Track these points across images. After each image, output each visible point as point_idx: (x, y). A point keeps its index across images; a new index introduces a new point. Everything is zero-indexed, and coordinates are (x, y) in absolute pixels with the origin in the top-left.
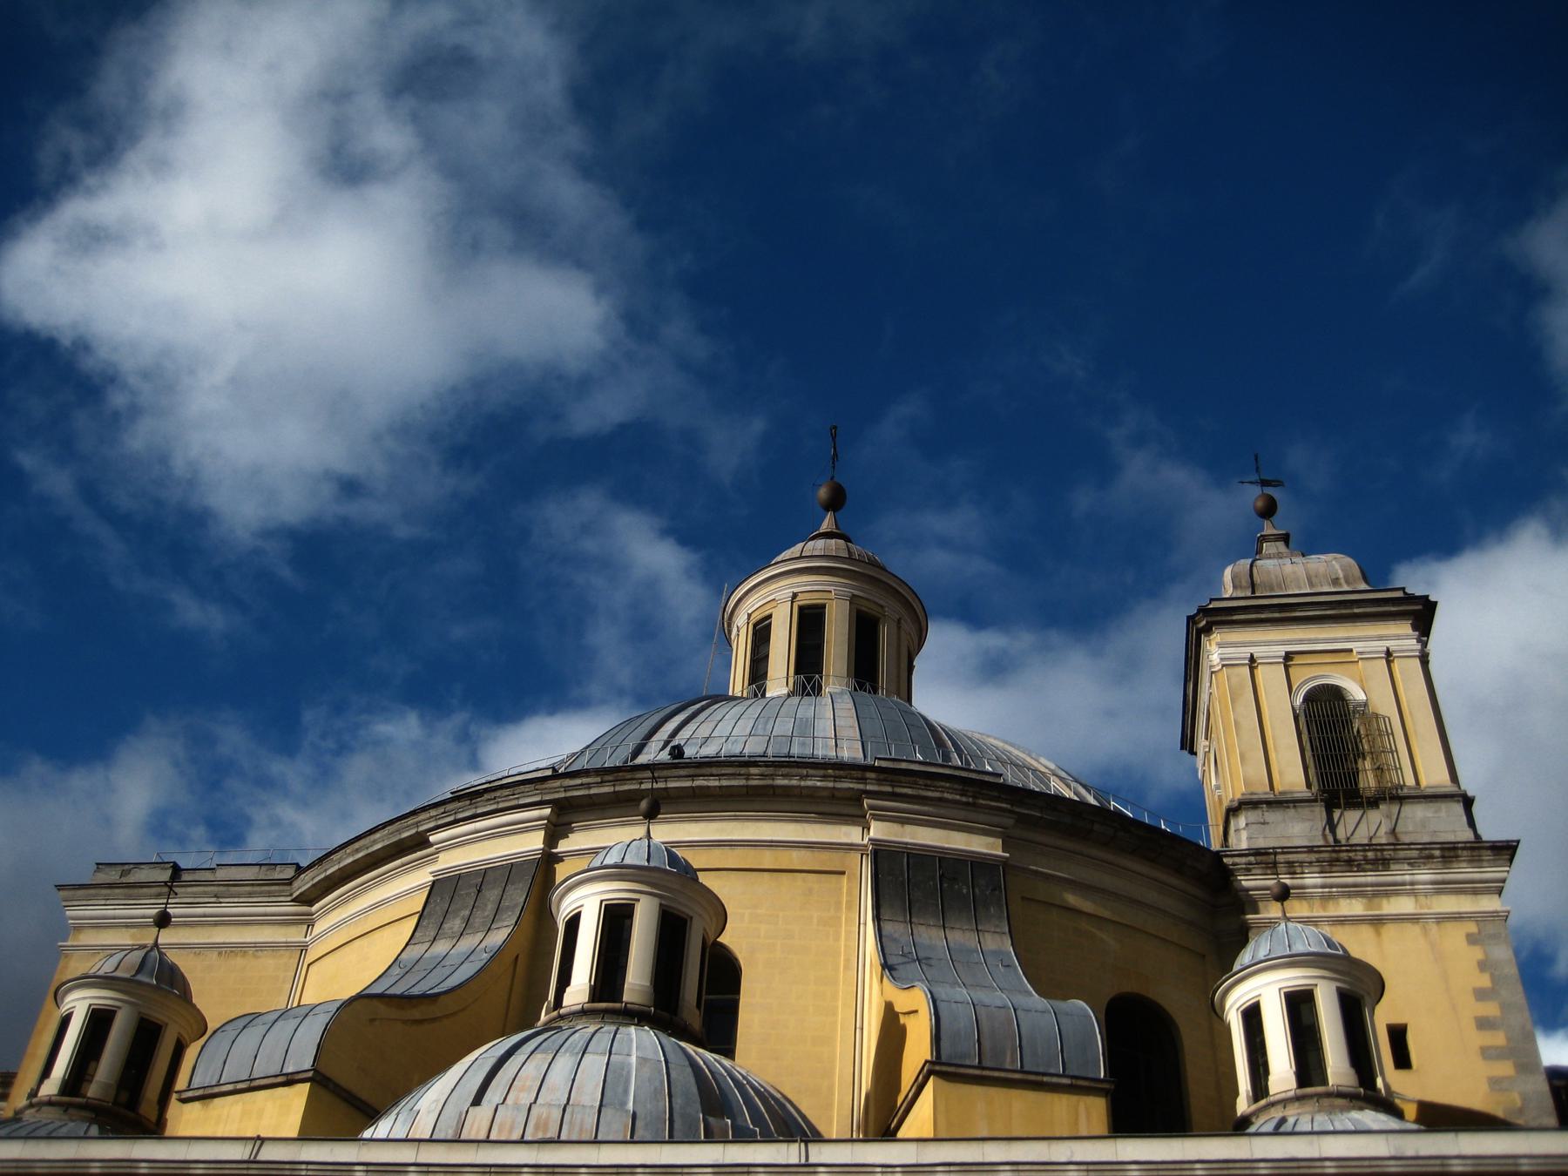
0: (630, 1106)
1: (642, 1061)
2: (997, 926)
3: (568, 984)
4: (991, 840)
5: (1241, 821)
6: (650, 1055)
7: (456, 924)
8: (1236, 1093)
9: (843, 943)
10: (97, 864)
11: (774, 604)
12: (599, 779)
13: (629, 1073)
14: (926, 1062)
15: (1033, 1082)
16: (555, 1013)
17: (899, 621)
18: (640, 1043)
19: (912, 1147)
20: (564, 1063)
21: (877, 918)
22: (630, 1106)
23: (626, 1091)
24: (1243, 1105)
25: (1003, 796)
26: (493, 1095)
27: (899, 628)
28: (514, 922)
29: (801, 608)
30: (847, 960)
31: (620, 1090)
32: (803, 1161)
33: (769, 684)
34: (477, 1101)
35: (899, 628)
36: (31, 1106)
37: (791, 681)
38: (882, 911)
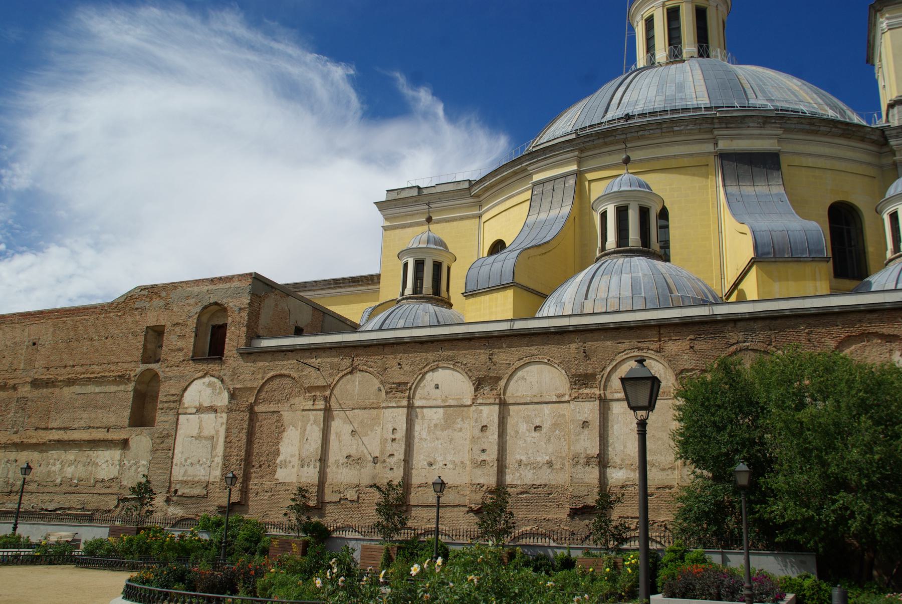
0: (643, 295)
1: (644, 275)
2: (777, 182)
3: (606, 240)
4: (772, 141)
5: (896, 110)
6: (646, 272)
7: (546, 205)
8: (886, 249)
9: (710, 196)
10: (387, 191)
11: (654, 8)
12: (597, 137)
13: (640, 280)
14: (752, 258)
15: (798, 261)
16: (603, 253)
17: (717, 6)
18: (641, 263)
19: (751, 305)
20: (615, 279)
21: (724, 185)
22: (643, 295)
23: (640, 288)
24: (889, 255)
25: (777, 121)
26: (591, 295)
27: (717, 9)
28: (571, 203)
29: (668, 9)
30: (713, 204)
31: (638, 288)
32: (711, 314)
33: (656, 52)
34: (586, 298)
35: (717, 9)
36: (403, 299)
37: (667, 50)
38: (726, 182)
